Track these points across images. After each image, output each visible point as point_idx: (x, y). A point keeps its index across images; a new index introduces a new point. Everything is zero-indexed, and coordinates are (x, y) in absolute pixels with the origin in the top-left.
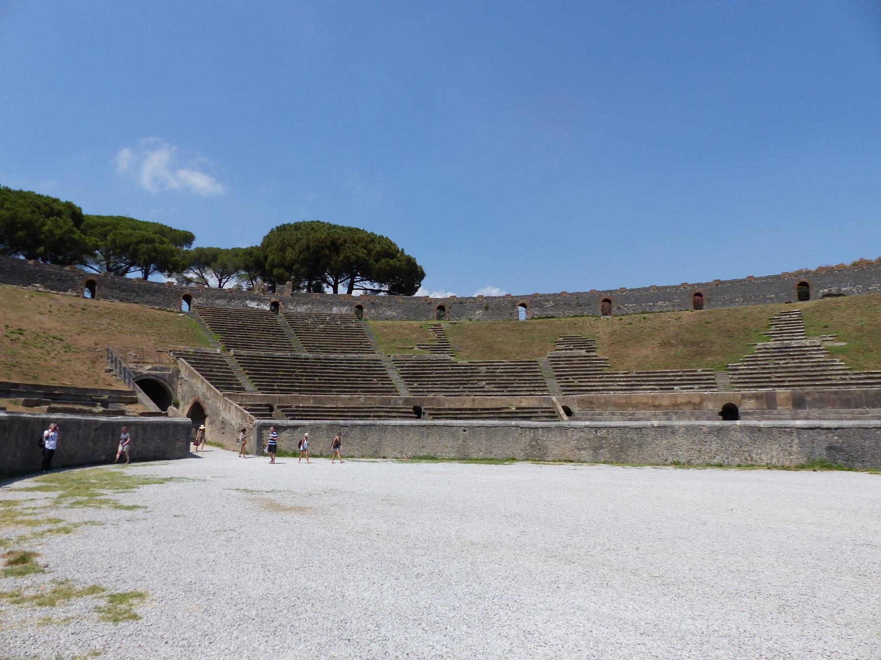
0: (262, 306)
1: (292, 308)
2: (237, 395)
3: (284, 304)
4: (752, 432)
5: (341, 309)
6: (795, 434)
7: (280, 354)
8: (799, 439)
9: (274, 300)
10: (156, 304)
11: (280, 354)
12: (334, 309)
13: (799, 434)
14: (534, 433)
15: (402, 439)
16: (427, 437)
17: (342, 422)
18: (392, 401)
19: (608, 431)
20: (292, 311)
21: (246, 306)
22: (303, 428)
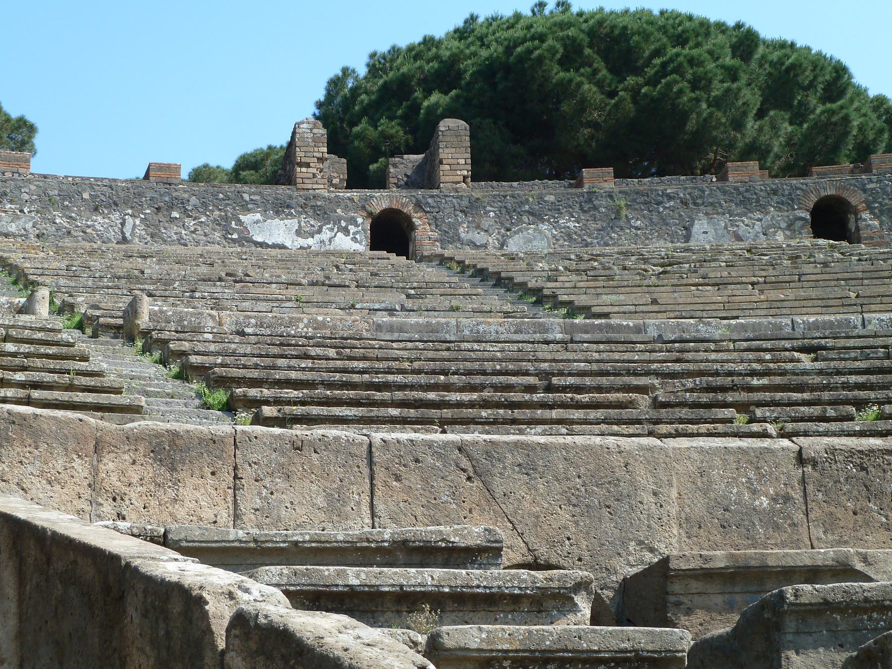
0: (326, 234)
1: (479, 237)
3: (436, 223)
5: (742, 229)
9: (385, 205)
12: (700, 226)
21: (245, 240)
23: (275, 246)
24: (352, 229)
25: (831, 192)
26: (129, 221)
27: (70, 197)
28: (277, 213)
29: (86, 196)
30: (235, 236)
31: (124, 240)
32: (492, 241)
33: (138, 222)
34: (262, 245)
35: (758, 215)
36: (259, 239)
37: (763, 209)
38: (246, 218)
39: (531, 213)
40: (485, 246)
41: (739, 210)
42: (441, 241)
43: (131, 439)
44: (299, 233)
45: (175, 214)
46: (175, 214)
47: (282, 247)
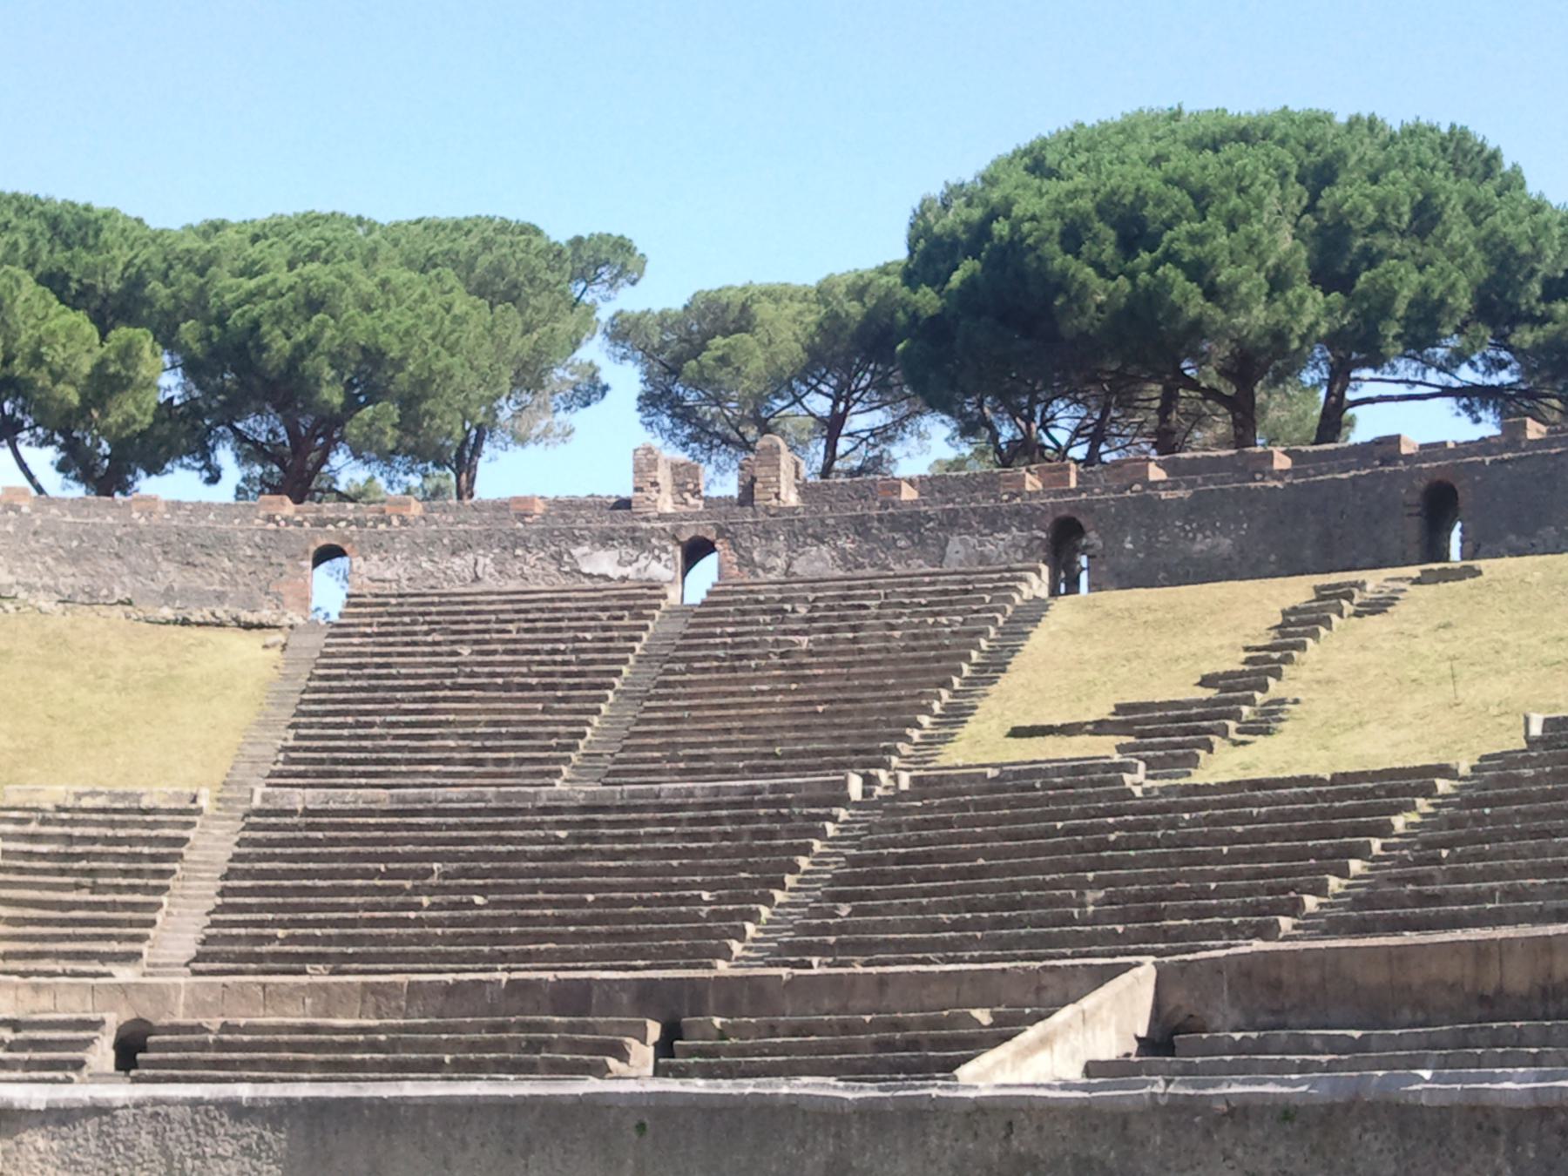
0: (642, 562)
2: (17, 987)
3: (735, 547)
4: (1403, 1131)
6: (1502, 1143)
7: (453, 793)
8: (1513, 1163)
10: (201, 598)
11: (453, 793)
13: (1514, 1141)
14: (838, 1135)
15: (446, 1163)
16: (525, 1155)
17: (244, 1091)
18: (596, 990)
19: (1040, 1128)
20: (772, 577)
22: (105, 1119)
23: (601, 576)
24: (664, 556)
25: (1064, 512)
26: (481, 560)
27: (432, 543)
28: (603, 545)
29: (446, 541)
30: (567, 569)
31: (477, 579)
32: (780, 562)
33: (488, 561)
34: (590, 576)
35: (1002, 535)
36: (586, 570)
37: (1006, 529)
38: (577, 552)
39: (814, 536)
40: (773, 568)
41: (987, 531)
42: (738, 564)
43: (26, 984)
44: (620, 563)
45: (519, 552)
46: (519, 552)
47: (606, 578)
